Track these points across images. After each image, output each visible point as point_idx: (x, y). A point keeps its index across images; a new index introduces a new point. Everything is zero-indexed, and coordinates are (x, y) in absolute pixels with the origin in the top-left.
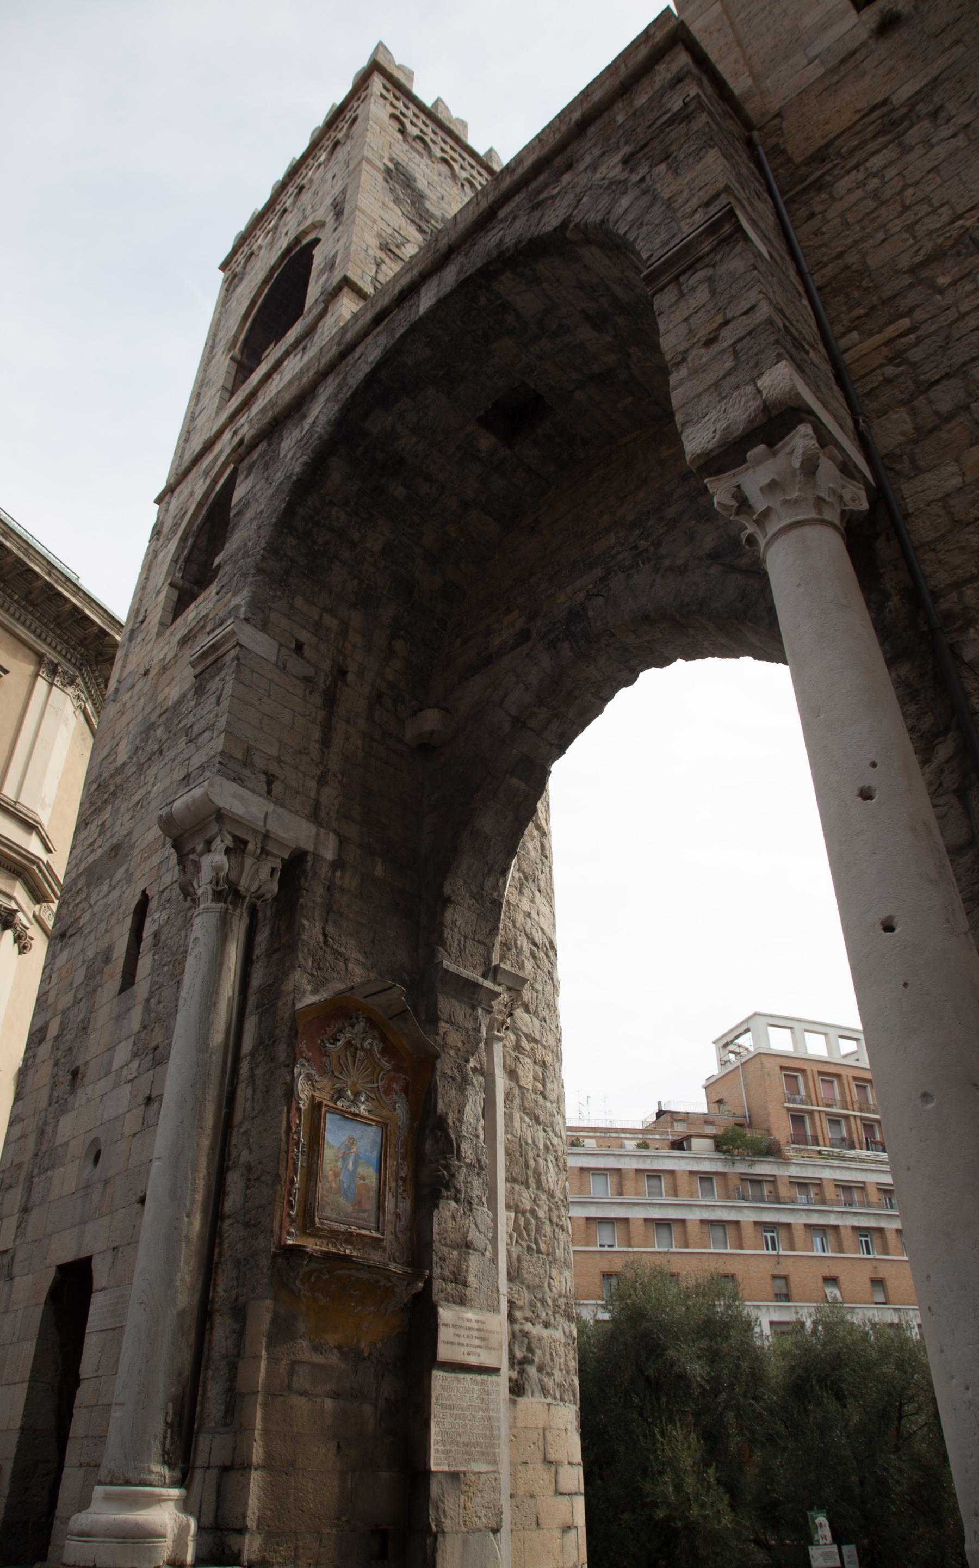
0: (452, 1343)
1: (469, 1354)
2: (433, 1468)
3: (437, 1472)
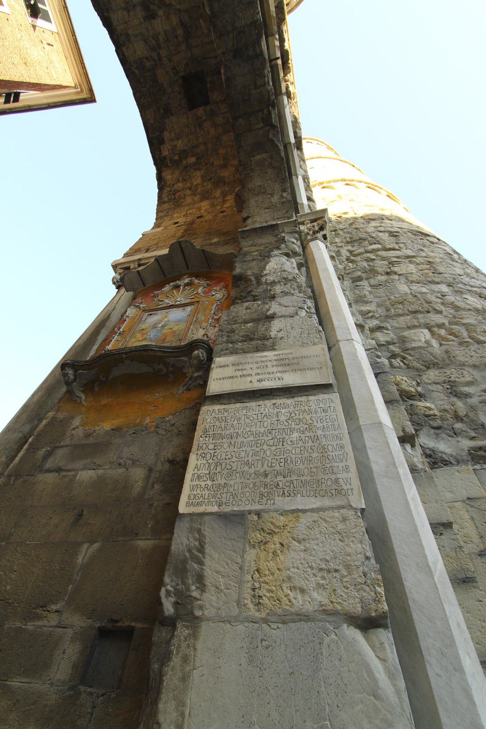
2: (182, 508)
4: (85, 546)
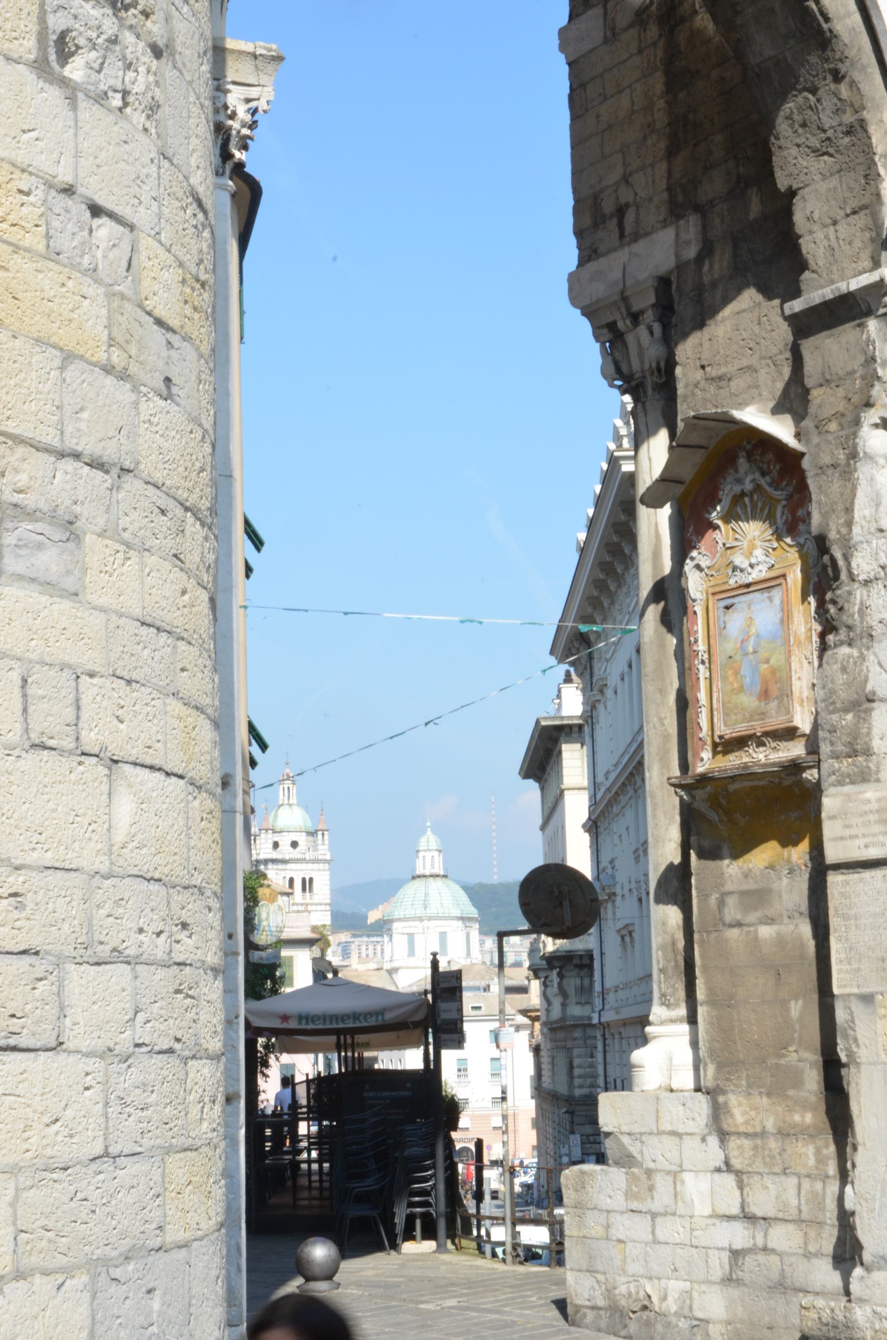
0: (842, 838)
1: (866, 846)
2: (836, 990)
3: (842, 995)
4: (793, 1003)
